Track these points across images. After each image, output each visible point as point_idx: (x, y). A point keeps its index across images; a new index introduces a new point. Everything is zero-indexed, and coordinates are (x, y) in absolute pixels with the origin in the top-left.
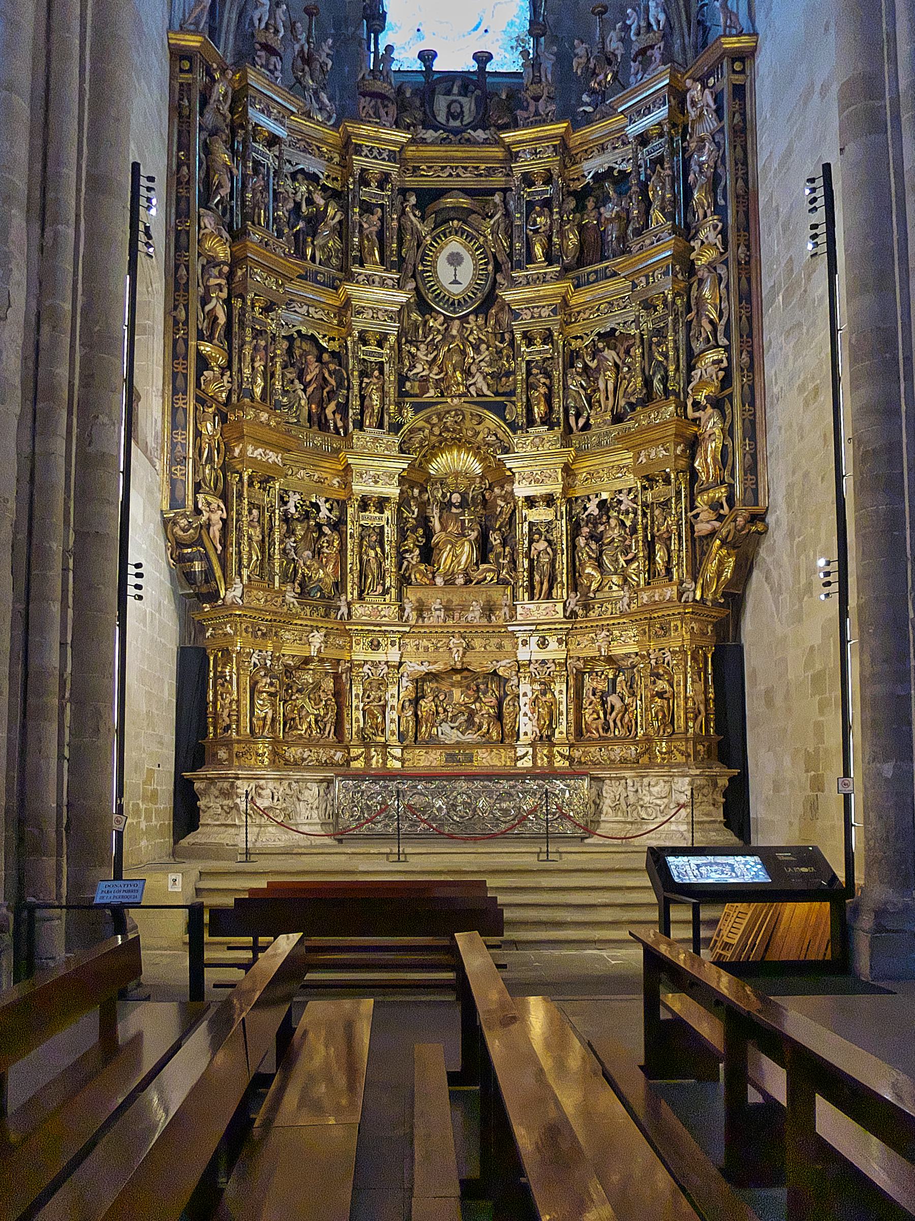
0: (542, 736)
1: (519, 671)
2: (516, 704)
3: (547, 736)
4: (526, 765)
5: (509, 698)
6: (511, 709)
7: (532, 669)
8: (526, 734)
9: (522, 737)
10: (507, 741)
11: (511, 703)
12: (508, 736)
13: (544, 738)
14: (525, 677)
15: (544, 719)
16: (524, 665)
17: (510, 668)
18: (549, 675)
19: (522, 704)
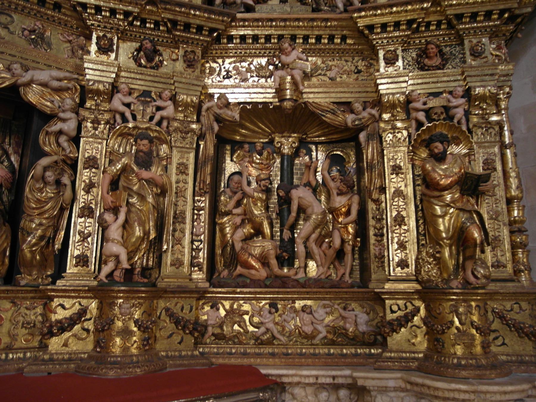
0: (129, 273)
1: (82, 103)
2: (66, 180)
3: (145, 270)
4: (75, 346)
5: (45, 161)
6: (50, 192)
7: (117, 103)
8: (83, 260)
9: (71, 269)
10: (24, 279)
11: (50, 176)
12: (30, 265)
13: (137, 278)
14: (96, 122)
15: (142, 224)
16: (98, 93)
17: (58, 90)
18: (159, 124)
19: (80, 186)
